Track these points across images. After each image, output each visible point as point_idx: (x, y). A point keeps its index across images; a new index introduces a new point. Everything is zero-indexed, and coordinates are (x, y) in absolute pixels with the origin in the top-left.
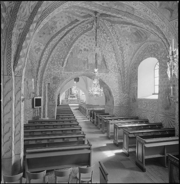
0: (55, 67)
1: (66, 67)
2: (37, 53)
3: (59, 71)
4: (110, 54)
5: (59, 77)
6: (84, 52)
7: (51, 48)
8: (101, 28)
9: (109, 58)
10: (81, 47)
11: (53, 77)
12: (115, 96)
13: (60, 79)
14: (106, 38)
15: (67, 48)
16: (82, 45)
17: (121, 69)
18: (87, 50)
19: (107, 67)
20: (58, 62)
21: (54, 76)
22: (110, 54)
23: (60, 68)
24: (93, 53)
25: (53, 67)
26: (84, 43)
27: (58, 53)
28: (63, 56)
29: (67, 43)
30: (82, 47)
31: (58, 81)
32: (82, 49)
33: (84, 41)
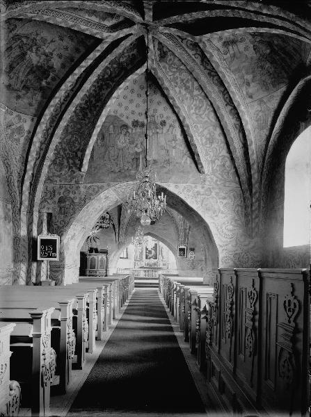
0: (63, 172)
1: (88, 172)
2: (18, 140)
3: (73, 182)
4: (206, 132)
5: (72, 195)
6: (134, 131)
8: (172, 57)
9: (204, 141)
10: (124, 119)
12: (221, 244)
14: (190, 84)
15: (89, 123)
16: (125, 113)
19: (199, 166)
24: (158, 130)
25: (59, 173)
26: (132, 107)
27: (70, 137)
28: (80, 144)
30: (127, 118)
33: (131, 101)
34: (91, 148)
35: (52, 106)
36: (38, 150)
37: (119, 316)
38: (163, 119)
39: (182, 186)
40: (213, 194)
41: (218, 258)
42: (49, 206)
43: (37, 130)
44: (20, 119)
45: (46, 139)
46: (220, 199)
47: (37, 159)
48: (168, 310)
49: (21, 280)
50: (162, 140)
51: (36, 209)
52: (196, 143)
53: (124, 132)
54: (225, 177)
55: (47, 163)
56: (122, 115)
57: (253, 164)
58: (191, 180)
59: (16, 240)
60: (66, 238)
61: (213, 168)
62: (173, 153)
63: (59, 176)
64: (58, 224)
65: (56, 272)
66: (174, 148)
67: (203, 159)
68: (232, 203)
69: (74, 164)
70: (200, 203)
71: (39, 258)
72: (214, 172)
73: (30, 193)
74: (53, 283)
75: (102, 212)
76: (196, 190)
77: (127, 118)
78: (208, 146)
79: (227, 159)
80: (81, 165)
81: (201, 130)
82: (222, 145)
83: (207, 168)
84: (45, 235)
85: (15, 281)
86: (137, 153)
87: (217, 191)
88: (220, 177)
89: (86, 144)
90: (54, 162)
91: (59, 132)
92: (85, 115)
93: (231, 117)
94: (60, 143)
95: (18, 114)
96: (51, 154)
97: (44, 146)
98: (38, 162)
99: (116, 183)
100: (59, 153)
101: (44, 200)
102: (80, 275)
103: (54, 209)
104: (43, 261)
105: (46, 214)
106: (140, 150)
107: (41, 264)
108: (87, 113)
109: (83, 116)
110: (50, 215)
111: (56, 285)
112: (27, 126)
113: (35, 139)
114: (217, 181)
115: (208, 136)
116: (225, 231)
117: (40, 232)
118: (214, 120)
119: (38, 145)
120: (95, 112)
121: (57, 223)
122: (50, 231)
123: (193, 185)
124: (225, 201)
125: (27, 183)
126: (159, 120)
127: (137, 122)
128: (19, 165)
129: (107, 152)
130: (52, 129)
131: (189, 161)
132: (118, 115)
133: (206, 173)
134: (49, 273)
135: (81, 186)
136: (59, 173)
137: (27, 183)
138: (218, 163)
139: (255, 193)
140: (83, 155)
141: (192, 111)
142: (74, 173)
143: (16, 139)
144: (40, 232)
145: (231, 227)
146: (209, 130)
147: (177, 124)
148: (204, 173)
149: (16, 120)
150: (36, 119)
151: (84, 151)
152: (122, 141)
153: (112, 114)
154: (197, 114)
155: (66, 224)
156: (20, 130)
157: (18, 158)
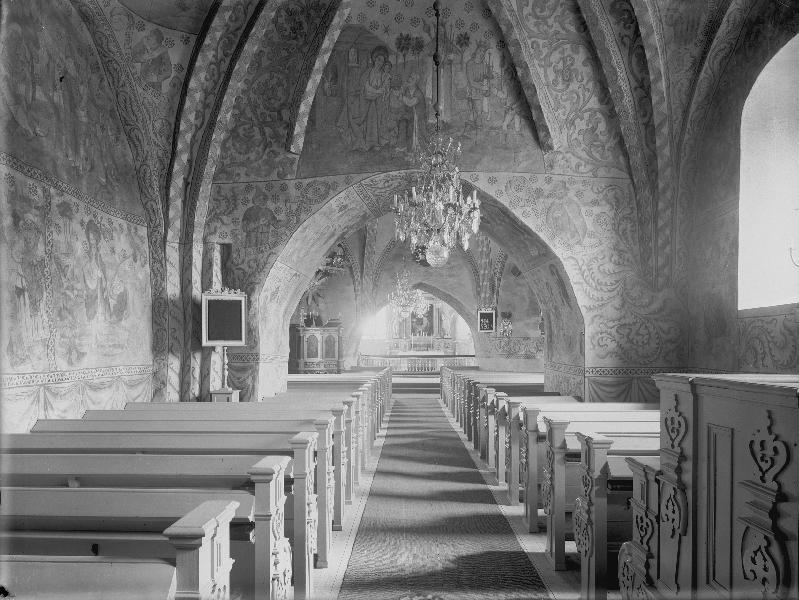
0: (252, 156)
2: (157, 86)
3: (274, 176)
4: (556, 56)
5: (271, 205)
6: (401, 60)
7: (226, 55)
9: (552, 77)
10: (378, 33)
11: (245, 209)
13: (281, 217)
15: (306, 43)
17: (632, 141)
18: (413, 43)
19: (542, 134)
20: (268, 130)
21: (251, 205)
22: (556, 56)
23: (277, 159)
25: (242, 158)
27: (266, 76)
29: (302, 18)
31: (272, 228)
32: (390, 41)
34: (310, 99)
35: (227, 9)
36: (200, 107)
37: (373, 463)
38: (463, 31)
39: (503, 176)
40: (571, 194)
41: (583, 334)
42: (224, 228)
43: (197, 64)
44: (160, 38)
45: (216, 83)
46: (585, 204)
47: (198, 129)
48: (470, 446)
49: (169, 388)
50: (461, 79)
51: (198, 235)
52: (535, 81)
53: (379, 62)
54: (598, 156)
55: (218, 136)
56: (374, 26)
57: (661, 125)
58: (524, 164)
59: (159, 307)
60: (261, 297)
61: (569, 137)
62: (485, 104)
63: (243, 164)
64: (245, 266)
65: (242, 369)
66: (487, 94)
67: (551, 117)
68: (611, 214)
69: (276, 136)
70: (543, 218)
71: (205, 342)
72: (570, 149)
73: (184, 202)
74: (236, 395)
75: (332, 241)
76: (534, 186)
77: (386, 30)
78: (560, 86)
79: (599, 115)
80: (290, 138)
81: (545, 51)
82: (590, 85)
83: (558, 139)
84: (219, 292)
85: (158, 392)
86: (408, 109)
87: (579, 186)
88: (584, 155)
89: (301, 92)
90: (233, 133)
91: (242, 66)
92: (297, 29)
93: (612, 20)
94: (244, 92)
95: (155, 27)
96: (226, 116)
97: (212, 100)
98: (200, 133)
99: (365, 175)
100: (242, 113)
101: (213, 216)
102: (291, 371)
103: (234, 234)
104: (213, 348)
105: (218, 247)
106: (415, 101)
107: (209, 355)
108: (300, 24)
109: (293, 30)
110: (226, 249)
111: (241, 400)
112: (176, 55)
113: (192, 84)
114: (578, 166)
115: (560, 66)
116: (598, 276)
117: (206, 285)
118: (573, 29)
119: (198, 96)
120: (318, 21)
121: (240, 275)
122: (227, 283)
123: (527, 176)
124: (596, 210)
125: (178, 182)
126: (454, 34)
127: (408, 38)
128: (162, 141)
129: (345, 109)
130: (228, 60)
131: (518, 122)
132: (367, 25)
133: (556, 147)
134: (227, 373)
135: (291, 184)
136: (242, 158)
137: (178, 182)
138: (581, 125)
139: (664, 191)
140: (294, 116)
141: (527, 10)
142: (276, 154)
143: (153, 85)
144: (206, 285)
145: (609, 267)
146: (562, 52)
147: (493, 43)
148: (551, 148)
149: (153, 40)
150: (193, 39)
151: (294, 105)
152: (374, 84)
153: (355, 22)
154: (538, 18)
155: (261, 268)
156: (161, 62)
157: (158, 125)
